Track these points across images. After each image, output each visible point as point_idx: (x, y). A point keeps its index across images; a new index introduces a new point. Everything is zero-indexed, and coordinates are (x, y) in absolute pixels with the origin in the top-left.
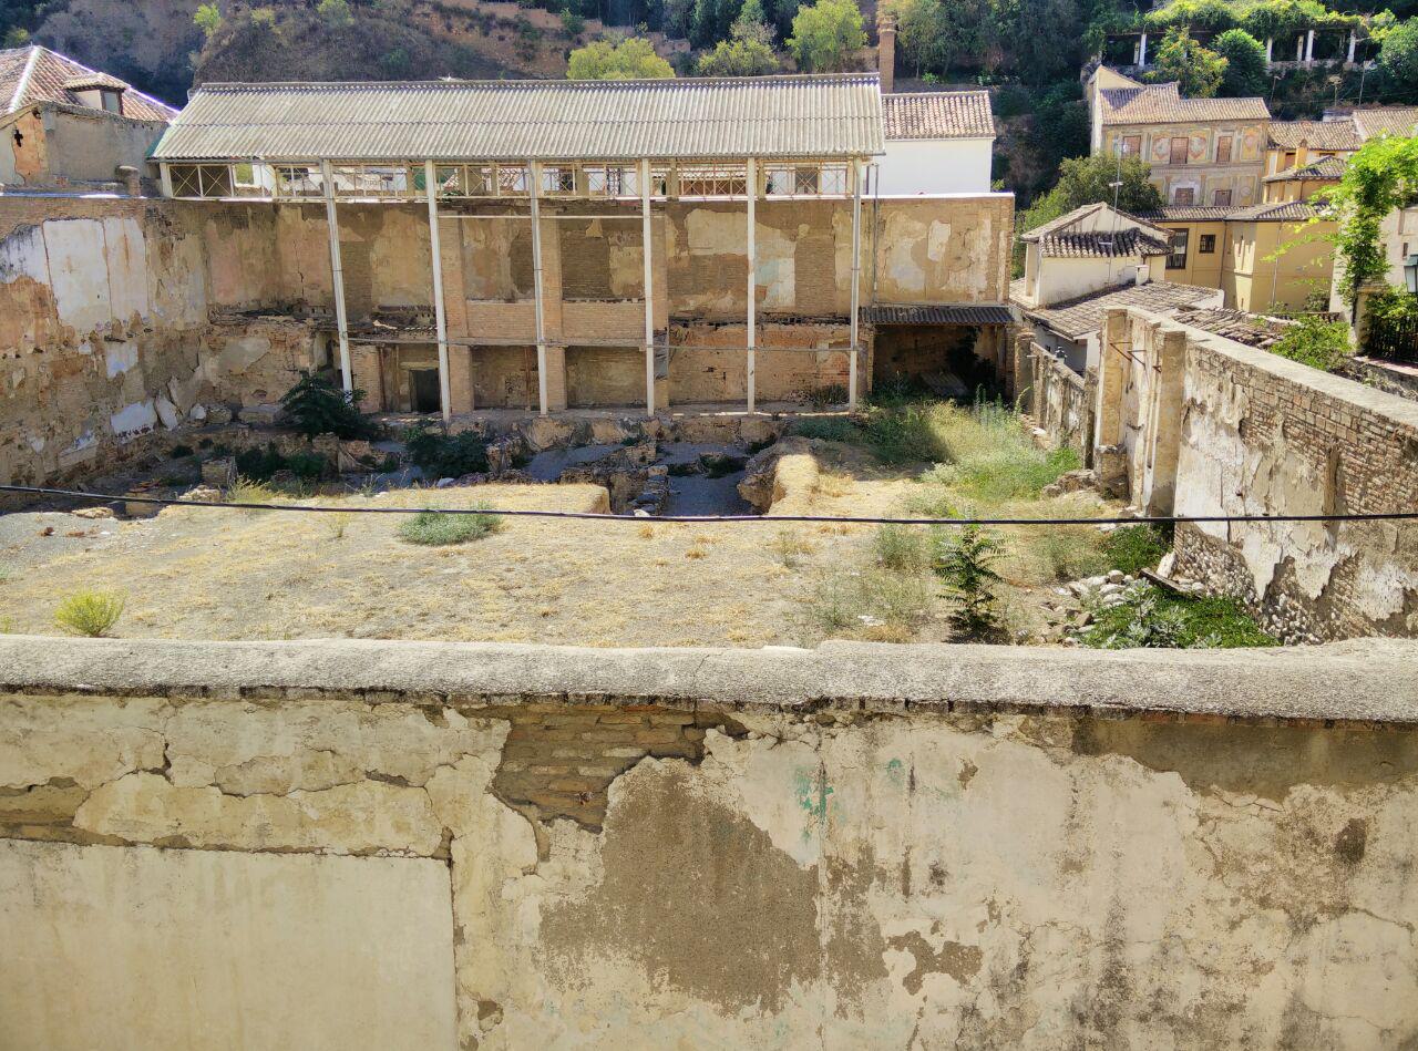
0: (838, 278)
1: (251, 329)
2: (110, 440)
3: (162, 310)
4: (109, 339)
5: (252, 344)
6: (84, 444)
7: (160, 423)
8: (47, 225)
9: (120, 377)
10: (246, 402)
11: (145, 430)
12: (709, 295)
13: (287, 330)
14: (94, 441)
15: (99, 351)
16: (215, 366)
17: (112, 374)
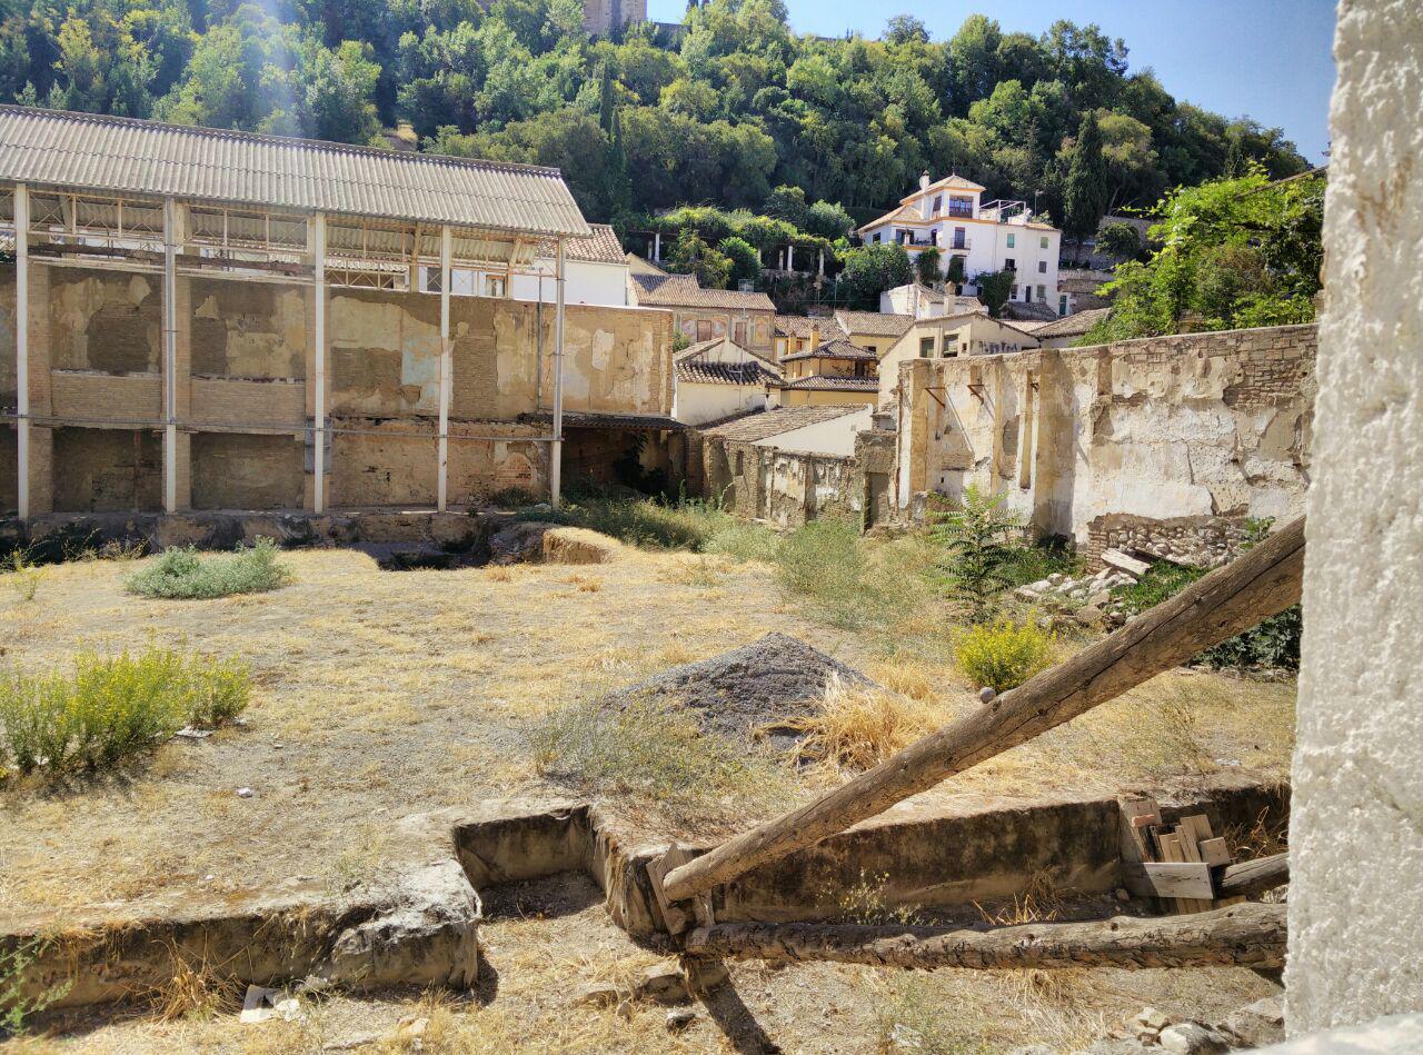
0: (500, 382)
12: (353, 393)
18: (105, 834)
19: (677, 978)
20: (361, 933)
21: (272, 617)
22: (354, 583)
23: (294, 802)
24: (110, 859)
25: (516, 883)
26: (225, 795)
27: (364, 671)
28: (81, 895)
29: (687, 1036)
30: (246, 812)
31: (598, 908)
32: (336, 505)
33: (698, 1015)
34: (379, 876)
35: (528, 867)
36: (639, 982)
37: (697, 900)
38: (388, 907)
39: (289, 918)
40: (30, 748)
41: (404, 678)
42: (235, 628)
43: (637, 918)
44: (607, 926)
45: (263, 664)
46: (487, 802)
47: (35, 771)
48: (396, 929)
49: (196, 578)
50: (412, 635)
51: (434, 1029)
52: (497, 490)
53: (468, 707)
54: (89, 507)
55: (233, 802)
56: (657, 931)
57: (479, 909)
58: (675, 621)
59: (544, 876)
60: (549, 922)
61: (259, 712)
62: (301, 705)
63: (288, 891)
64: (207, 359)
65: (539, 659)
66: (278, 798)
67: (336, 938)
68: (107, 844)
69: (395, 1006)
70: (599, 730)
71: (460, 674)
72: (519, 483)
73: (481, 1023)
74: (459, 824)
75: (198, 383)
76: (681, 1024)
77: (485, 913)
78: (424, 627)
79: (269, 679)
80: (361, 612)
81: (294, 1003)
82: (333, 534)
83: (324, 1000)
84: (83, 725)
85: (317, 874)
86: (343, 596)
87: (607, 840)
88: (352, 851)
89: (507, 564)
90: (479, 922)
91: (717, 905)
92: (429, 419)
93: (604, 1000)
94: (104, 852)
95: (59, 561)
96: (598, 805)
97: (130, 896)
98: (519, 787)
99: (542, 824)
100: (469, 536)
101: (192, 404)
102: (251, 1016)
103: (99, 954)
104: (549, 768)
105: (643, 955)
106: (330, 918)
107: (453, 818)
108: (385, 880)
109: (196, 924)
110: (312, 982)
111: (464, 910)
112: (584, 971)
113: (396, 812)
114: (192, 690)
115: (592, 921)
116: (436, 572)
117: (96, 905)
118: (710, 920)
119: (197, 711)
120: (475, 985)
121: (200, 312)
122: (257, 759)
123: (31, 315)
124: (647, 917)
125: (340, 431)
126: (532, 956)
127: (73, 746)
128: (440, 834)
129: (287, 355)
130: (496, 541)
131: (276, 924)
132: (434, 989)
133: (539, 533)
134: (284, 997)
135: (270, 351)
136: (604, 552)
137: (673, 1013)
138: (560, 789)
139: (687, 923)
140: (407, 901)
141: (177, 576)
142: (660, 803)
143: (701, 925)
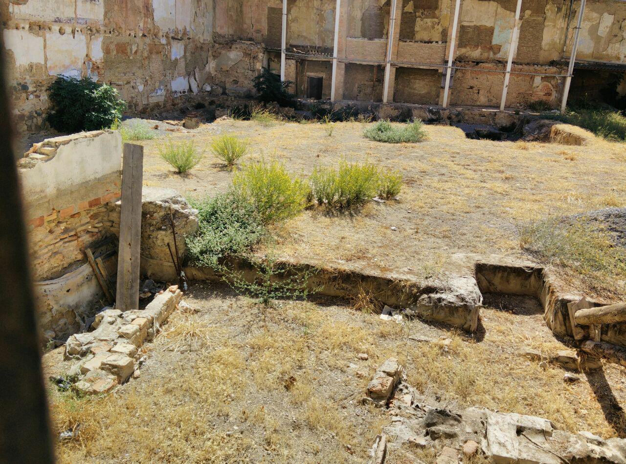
1: (234, 46)
2: (170, 93)
3: (195, 29)
4: (173, 38)
5: (234, 55)
6: (159, 93)
7: (190, 90)
9: (176, 60)
10: (228, 86)
11: (184, 92)
13: (252, 48)
14: (163, 92)
15: (169, 44)
16: (214, 65)
17: (173, 58)
18: (342, 234)
19: (574, 360)
20: (429, 297)
21: (416, 154)
22: (452, 143)
23: (412, 237)
24: (342, 244)
25: (501, 294)
26: (386, 228)
27: (450, 185)
28: (331, 255)
29: (573, 387)
30: (393, 237)
31: (540, 316)
32: (452, 104)
33: (581, 379)
34: (440, 276)
35: (511, 289)
36: (553, 355)
37: (592, 327)
38: (442, 290)
39: (403, 284)
40: (322, 196)
41: (467, 191)
42: (401, 157)
43: (558, 327)
44: (543, 326)
45: (409, 175)
46: (493, 255)
47: (323, 205)
48: (444, 300)
49: (389, 134)
50: (475, 171)
51: (454, 345)
52: (532, 101)
53: (493, 209)
54: (355, 98)
55: (389, 232)
56: (568, 336)
57: (481, 301)
58: (616, 182)
59: (515, 295)
60: (514, 316)
61: (405, 195)
62: (422, 195)
63: (403, 272)
64: (407, 33)
65: (534, 192)
66: (406, 234)
67: (419, 296)
68: (343, 238)
69: (439, 331)
70: (556, 233)
71: (493, 193)
72: (545, 98)
73: (474, 349)
74: (479, 262)
75: (401, 43)
76: (571, 381)
77: (484, 303)
78: (480, 168)
79: (410, 182)
80: (454, 157)
81: (401, 317)
82: (449, 118)
83: (412, 319)
84: (340, 190)
85: (415, 270)
86: (447, 148)
87: (550, 287)
88: (430, 263)
89: (528, 141)
90: (480, 307)
91: (604, 331)
92: (503, 63)
93: (534, 358)
94: (341, 241)
95: (342, 121)
96: (547, 269)
97: (347, 260)
98: (510, 252)
99: (518, 272)
100: (513, 125)
101: (398, 54)
102: (384, 317)
103: (335, 279)
104: (526, 246)
105: (559, 344)
106: (418, 288)
107: (476, 259)
108: (442, 278)
109: (368, 277)
110: (408, 311)
111: (474, 300)
112: (526, 342)
113: (452, 250)
114: (380, 182)
115: (536, 321)
116: (492, 142)
117: (336, 260)
118: (598, 339)
119: (381, 191)
120: (475, 333)
121: (406, 9)
122: (401, 216)
123: (341, 13)
124: (564, 328)
125: (459, 68)
126: (503, 328)
127: (336, 198)
128: (469, 265)
129: (441, 30)
130: (527, 128)
131: (397, 285)
132: (456, 328)
133: (549, 126)
134: (397, 314)
135: (433, 28)
136: (584, 140)
137: (568, 375)
138: (530, 257)
139: (584, 336)
140: (450, 290)
141: (382, 132)
142: (582, 276)
143: (592, 339)
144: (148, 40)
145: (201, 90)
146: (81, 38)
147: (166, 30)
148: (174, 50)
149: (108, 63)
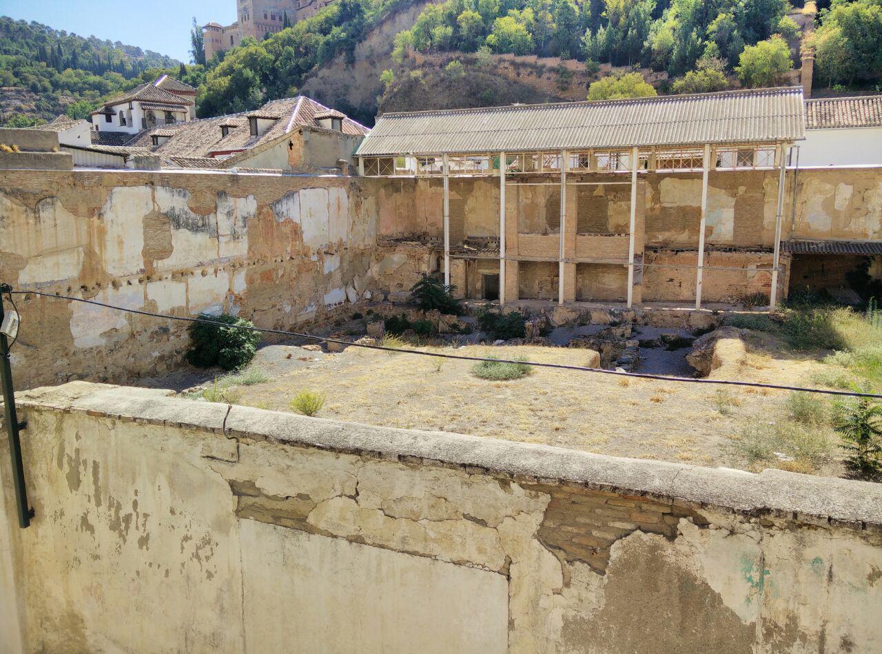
4: (326, 253)
6: (310, 309)
7: (347, 300)
8: (302, 191)
9: (330, 273)
11: (340, 303)
14: (314, 308)
17: (326, 272)
144: (296, 262)
145: (360, 297)
146: (224, 276)
147: (317, 247)
148: (326, 265)
149: (250, 292)
